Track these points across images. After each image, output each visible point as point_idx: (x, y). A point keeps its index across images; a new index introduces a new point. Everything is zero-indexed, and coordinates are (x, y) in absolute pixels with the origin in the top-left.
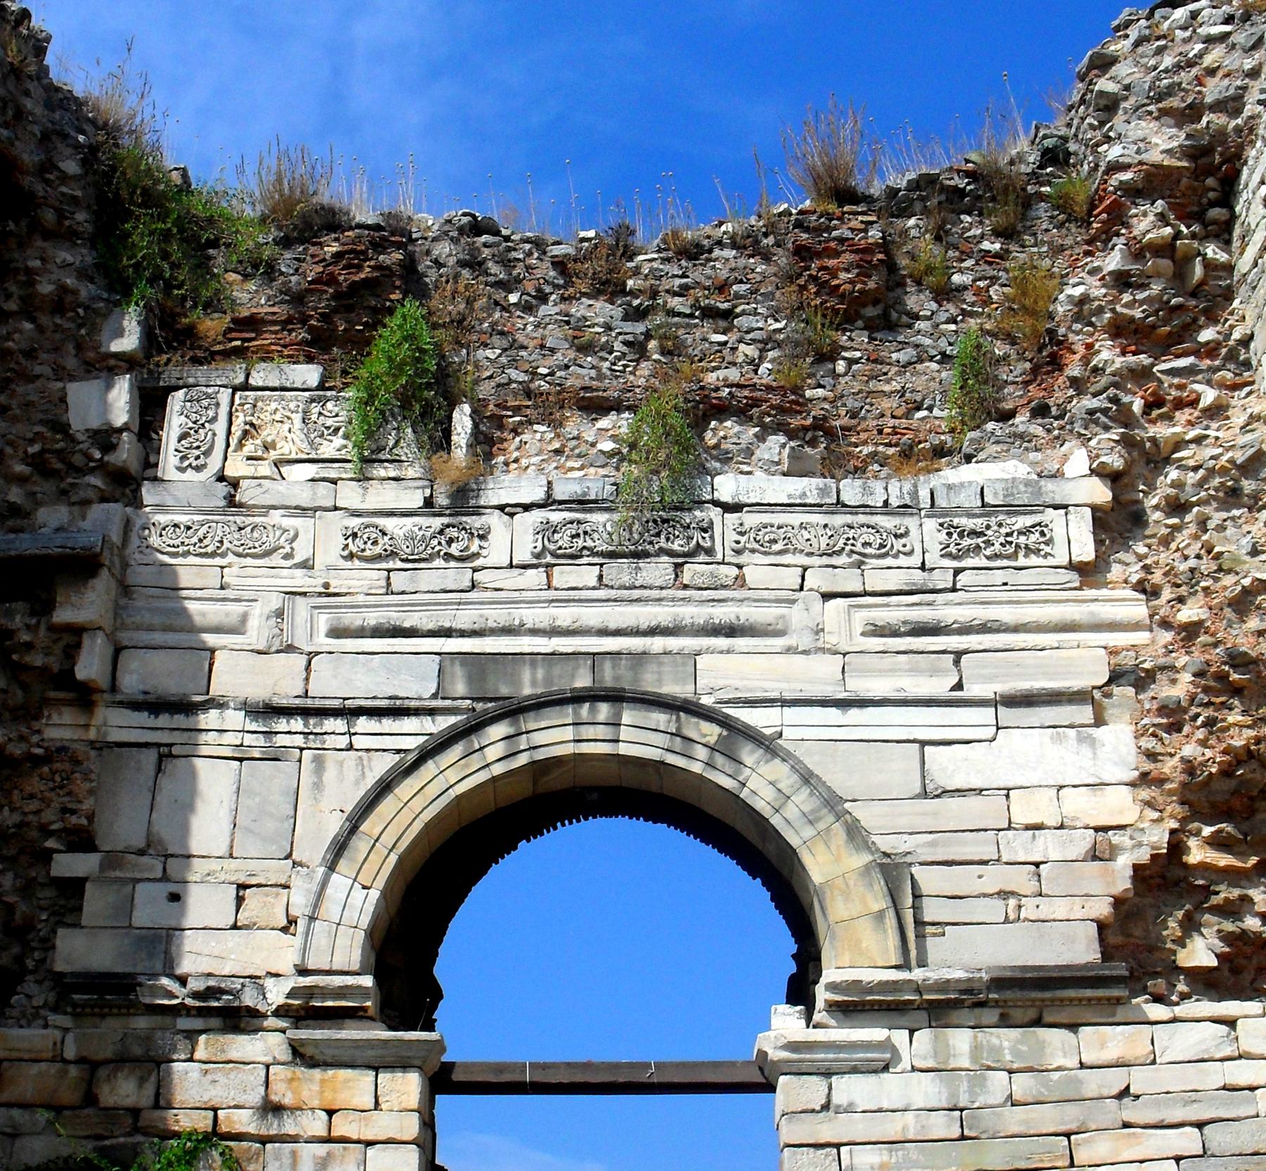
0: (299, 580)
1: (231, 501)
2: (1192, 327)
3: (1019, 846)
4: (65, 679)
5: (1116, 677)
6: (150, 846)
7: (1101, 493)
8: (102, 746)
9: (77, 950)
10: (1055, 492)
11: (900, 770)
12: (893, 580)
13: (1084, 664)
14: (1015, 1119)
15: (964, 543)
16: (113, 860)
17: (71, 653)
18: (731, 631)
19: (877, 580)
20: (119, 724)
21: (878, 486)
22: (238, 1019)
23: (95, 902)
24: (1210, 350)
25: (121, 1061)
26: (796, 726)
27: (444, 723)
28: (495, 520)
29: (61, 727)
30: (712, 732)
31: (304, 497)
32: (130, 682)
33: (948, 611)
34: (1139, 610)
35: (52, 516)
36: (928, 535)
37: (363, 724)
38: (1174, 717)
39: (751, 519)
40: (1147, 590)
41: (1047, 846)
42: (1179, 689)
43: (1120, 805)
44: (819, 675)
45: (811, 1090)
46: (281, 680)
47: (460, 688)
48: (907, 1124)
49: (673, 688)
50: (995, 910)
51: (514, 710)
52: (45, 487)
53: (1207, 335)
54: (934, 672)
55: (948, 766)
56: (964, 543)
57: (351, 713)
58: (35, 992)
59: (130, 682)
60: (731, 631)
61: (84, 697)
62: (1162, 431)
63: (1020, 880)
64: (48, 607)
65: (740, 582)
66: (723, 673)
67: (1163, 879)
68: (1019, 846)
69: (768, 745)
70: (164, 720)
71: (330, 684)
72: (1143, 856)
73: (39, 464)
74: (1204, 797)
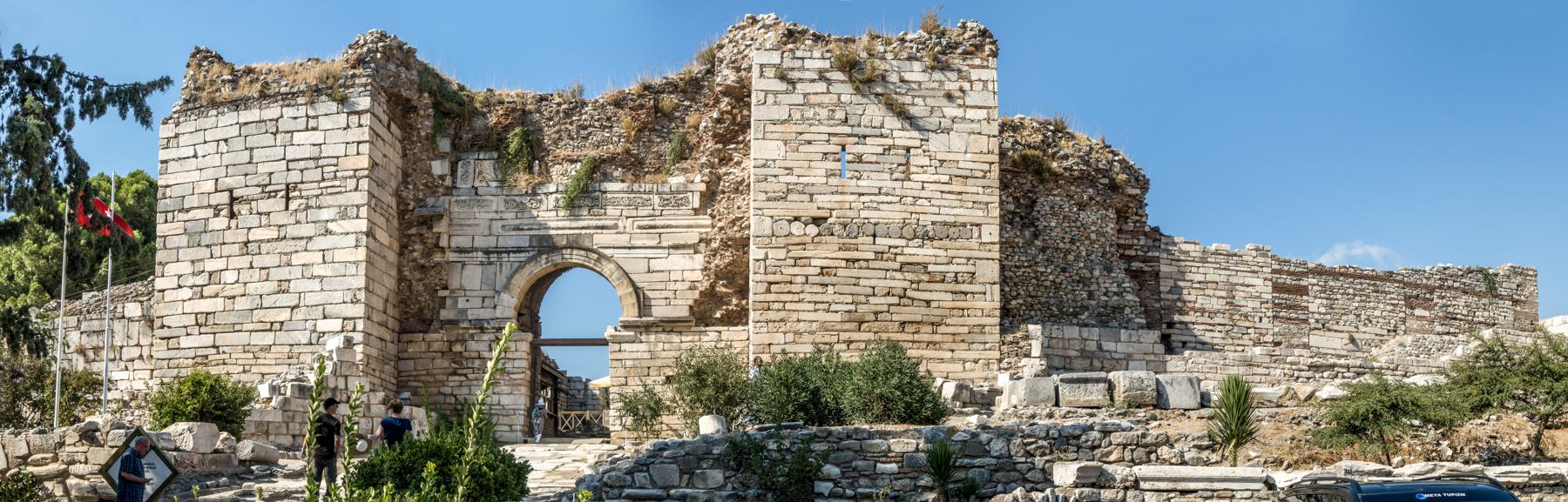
0: (494, 216)
2: (735, 137)
3: (672, 286)
4: (437, 245)
5: (701, 241)
6: (462, 288)
7: (703, 187)
8: (449, 263)
9: (445, 314)
10: (691, 187)
11: (643, 266)
12: (645, 213)
13: (692, 237)
14: (664, 354)
15: (665, 203)
16: (452, 291)
17: (438, 238)
18: (603, 228)
20: (452, 256)
22: (482, 330)
23: (448, 302)
25: (457, 341)
26: (617, 254)
29: (437, 258)
31: (494, 191)
32: (453, 245)
34: (709, 222)
35: (430, 201)
36: (656, 199)
38: (715, 253)
40: (713, 217)
41: (679, 286)
43: (698, 275)
44: (623, 240)
45: (617, 347)
46: (491, 242)
48: (639, 355)
49: (587, 244)
50: (664, 302)
52: (427, 192)
55: (655, 265)
56: (665, 203)
58: (436, 324)
59: (453, 245)
60: (603, 228)
61: (443, 250)
62: (723, 170)
63: (670, 295)
64: (430, 228)
66: (600, 239)
67: (710, 296)
68: (672, 286)
69: (609, 259)
71: (502, 243)
73: (426, 185)
74: (722, 274)
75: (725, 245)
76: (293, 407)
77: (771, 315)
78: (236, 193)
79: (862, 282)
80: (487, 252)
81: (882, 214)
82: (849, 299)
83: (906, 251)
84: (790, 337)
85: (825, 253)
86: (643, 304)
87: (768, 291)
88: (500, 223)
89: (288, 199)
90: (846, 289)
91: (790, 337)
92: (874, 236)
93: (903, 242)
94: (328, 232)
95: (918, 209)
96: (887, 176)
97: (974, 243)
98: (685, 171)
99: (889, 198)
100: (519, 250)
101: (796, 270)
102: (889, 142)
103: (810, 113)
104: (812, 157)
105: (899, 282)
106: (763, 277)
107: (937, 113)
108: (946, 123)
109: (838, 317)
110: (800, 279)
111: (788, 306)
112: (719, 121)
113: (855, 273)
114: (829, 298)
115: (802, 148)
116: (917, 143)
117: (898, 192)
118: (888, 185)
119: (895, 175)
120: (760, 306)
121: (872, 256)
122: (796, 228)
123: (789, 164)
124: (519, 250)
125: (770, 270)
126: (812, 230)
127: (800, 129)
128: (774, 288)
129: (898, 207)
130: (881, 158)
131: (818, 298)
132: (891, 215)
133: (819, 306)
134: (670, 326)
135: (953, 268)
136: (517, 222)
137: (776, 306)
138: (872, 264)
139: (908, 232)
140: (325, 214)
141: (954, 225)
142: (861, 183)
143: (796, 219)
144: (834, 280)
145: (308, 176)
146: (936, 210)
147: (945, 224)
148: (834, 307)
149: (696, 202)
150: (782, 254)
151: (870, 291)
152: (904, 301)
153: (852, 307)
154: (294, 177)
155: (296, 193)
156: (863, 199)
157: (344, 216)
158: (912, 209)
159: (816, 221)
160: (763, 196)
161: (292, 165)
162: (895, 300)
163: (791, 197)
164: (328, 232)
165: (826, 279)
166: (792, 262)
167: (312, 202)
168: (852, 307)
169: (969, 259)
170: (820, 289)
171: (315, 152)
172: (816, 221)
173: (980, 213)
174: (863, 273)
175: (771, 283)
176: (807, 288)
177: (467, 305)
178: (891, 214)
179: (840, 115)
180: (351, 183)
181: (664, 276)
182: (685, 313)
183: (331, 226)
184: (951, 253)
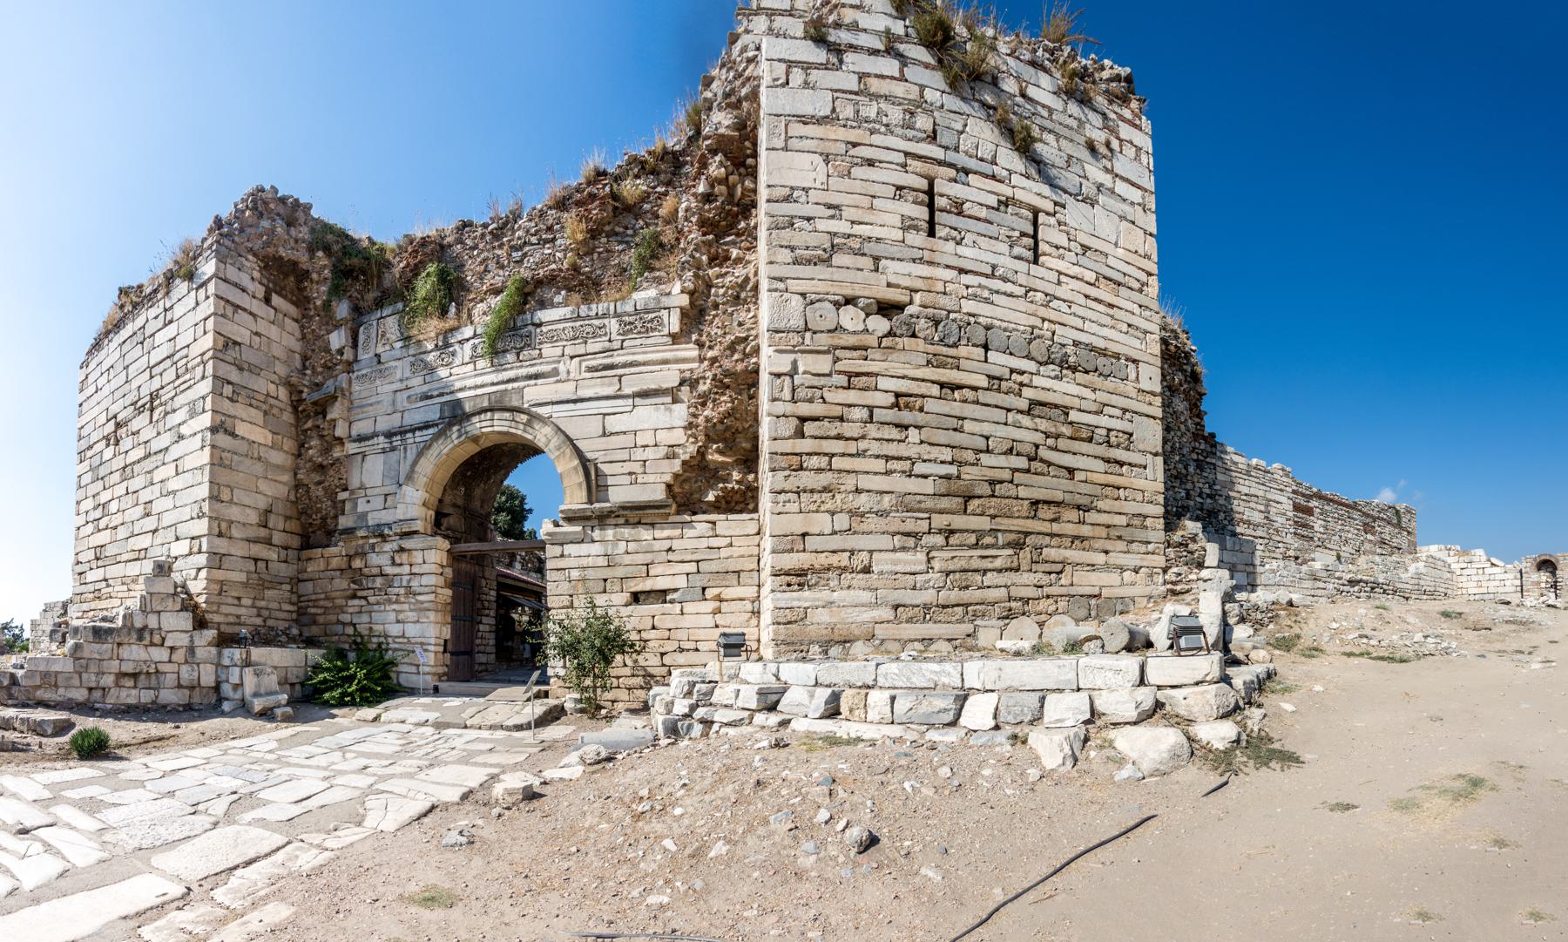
12: (598, 347)
21: (594, 306)
33: (617, 359)
43: (679, 436)
54: (610, 385)
72: (687, 457)
76: (86, 654)
77: (806, 479)
79: (968, 426)
81: (998, 312)
82: (947, 454)
83: (1037, 381)
84: (842, 521)
85: (903, 368)
86: (595, 483)
90: (942, 437)
91: (842, 521)
92: (986, 347)
93: (1030, 366)
95: (1053, 315)
96: (1004, 248)
97: (1129, 388)
98: (658, 281)
99: (1009, 287)
101: (851, 396)
102: (1008, 192)
105: (1027, 433)
106: (789, 408)
107: (1075, 168)
108: (1089, 189)
109: (928, 486)
110: (859, 414)
111: (837, 463)
112: (708, 198)
113: (956, 408)
114: (912, 451)
116: (1049, 207)
117: (1022, 279)
118: (1006, 263)
119: (1017, 250)
120: (783, 462)
121: (983, 382)
122: (850, 318)
125: (801, 393)
126: (880, 324)
128: (809, 428)
129: (1021, 304)
130: (993, 215)
131: (892, 449)
132: (1012, 316)
134: (636, 514)
135: (1103, 421)
137: (814, 462)
138: (984, 397)
139: (1038, 349)
141: (1103, 353)
142: (961, 250)
144: (920, 418)
147: (1093, 349)
148: (920, 468)
149: (674, 323)
150: (823, 364)
151: (981, 444)
153: (953, 470)
158: (1043, 312)
159: (887, 309)
160: (786, 256)
162: (1022, 463)
163: (838, 259)
165: (906, 417)
166: (843, 380)
168: (953, 470)
169: (1125, 411)
170: (894, 433)
172: (887, 309)
173: (1137, 343)
174: (970, 410)
175: (803, 420)
176: (872, 430)
178: (1011, 314)
181: (627, 440)
182: (659, 494)
184: (1102, 397)
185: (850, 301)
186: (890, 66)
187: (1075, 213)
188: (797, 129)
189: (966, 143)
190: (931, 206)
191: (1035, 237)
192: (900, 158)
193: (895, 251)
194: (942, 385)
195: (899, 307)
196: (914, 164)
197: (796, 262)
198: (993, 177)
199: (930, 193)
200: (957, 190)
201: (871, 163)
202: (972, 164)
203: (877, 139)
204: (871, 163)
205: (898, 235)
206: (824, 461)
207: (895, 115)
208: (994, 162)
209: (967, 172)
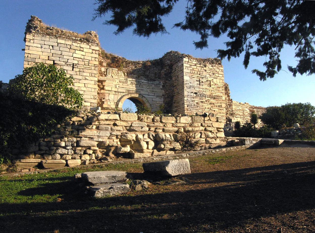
1: (112, 78)
5: (163, 95)
12: (151, 88)
16: (106, 100)
19: (150, 88)
24: (169, 76)
26: (146, 96)
27: (126, 94)
28: (129, 81)
30: (141, 96)
33: (154, 90)
37: (121, 93)
39: (144, 83)
42: (166, 96)
46: (116, 90)
47: (127, 92)
50: (155, 108)
51: (131, 93)
53: (169, 75)
57: (121, 93)
60: (142, 90)
65: (143, 87)
70: (109, 92)
71: (119, 90)
75: (168, 97)
78: (55, 62)
80: (116, 92)
81: (206, 93)
87: (188, 107)
88: (118, 86)
89: (73, 68)
92: (205, 97)
94: (86, 79)
99: (208, 90)
100: (123, 93)
101: (192, 103)
102: (207, 79)
103: (193, 72)
104: (194, 80)
115: (193, 79)
116: (211, 80)
121: (205, 101)
122: (192, 94)
123: (190, 81)
124: (123, 93)
126: (195, 95)
127: (192, 75)
129: (209, 92)
131: (196, 109)
133: (197, 110)
136: (123, 86)
138: (205, 103)
140: (85, 74)
143: (192, 92)
145: (80, 63)
146: (215, 93)
152: (211, 110)
154: (76, 62)
155: (76, 67)
156: (203, 90)
157: (92, 76)
159: (196, 93)
161: (75, 59)
164: (86, 79)
165: (198, 105)
166: (192, 101)
167: (81, 70)
170: (196, 107)
171: (82, 57)
172: (196, 93)
175: (188, 105)
177: (110, 104)
179: (199, 73)
180: (93, 68)
183: (87, 78)
185: (192, 92)
186: (195, 67)
187: (215, 80)
188: (187, 74)
189: (203, 75)
190: (199, 82)
191: (210, 84)
192: (197, 77)
193: (196, 87)
194: (201, 102)
195: (197, 93)
196: (198, 78)
197: (187, 88)
198: (206, 78)
199: (200, 81)
200: (202, 80)
201: (194, 78)
202: (203, 77)
203: (194, 75)
204: (194, 78)
205: (196, 85)
206: (190, 110)
207: (196, 73)
208: (206, 76)
209: (203, 78)
